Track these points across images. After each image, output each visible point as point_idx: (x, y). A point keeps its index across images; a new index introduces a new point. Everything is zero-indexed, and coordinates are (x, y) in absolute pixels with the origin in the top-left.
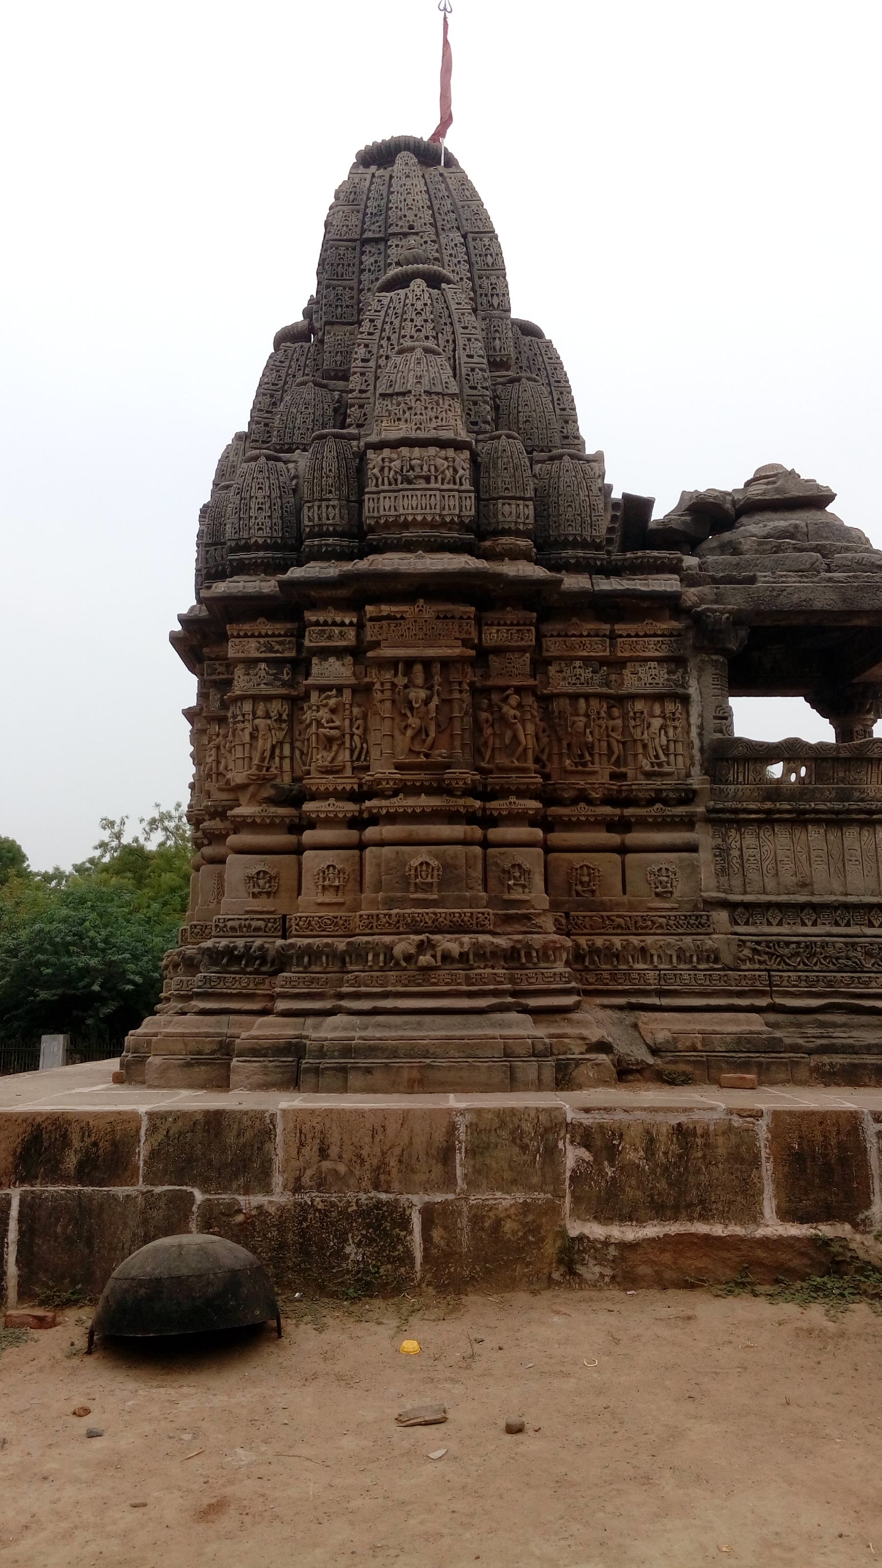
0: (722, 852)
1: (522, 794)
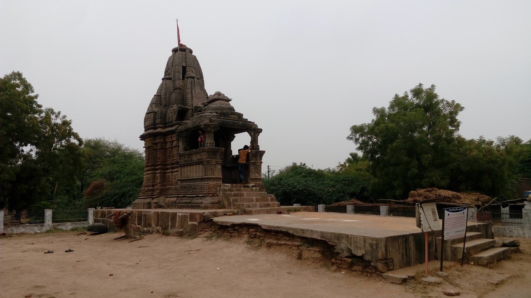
0: (181, 171)
1: (159, 165)
